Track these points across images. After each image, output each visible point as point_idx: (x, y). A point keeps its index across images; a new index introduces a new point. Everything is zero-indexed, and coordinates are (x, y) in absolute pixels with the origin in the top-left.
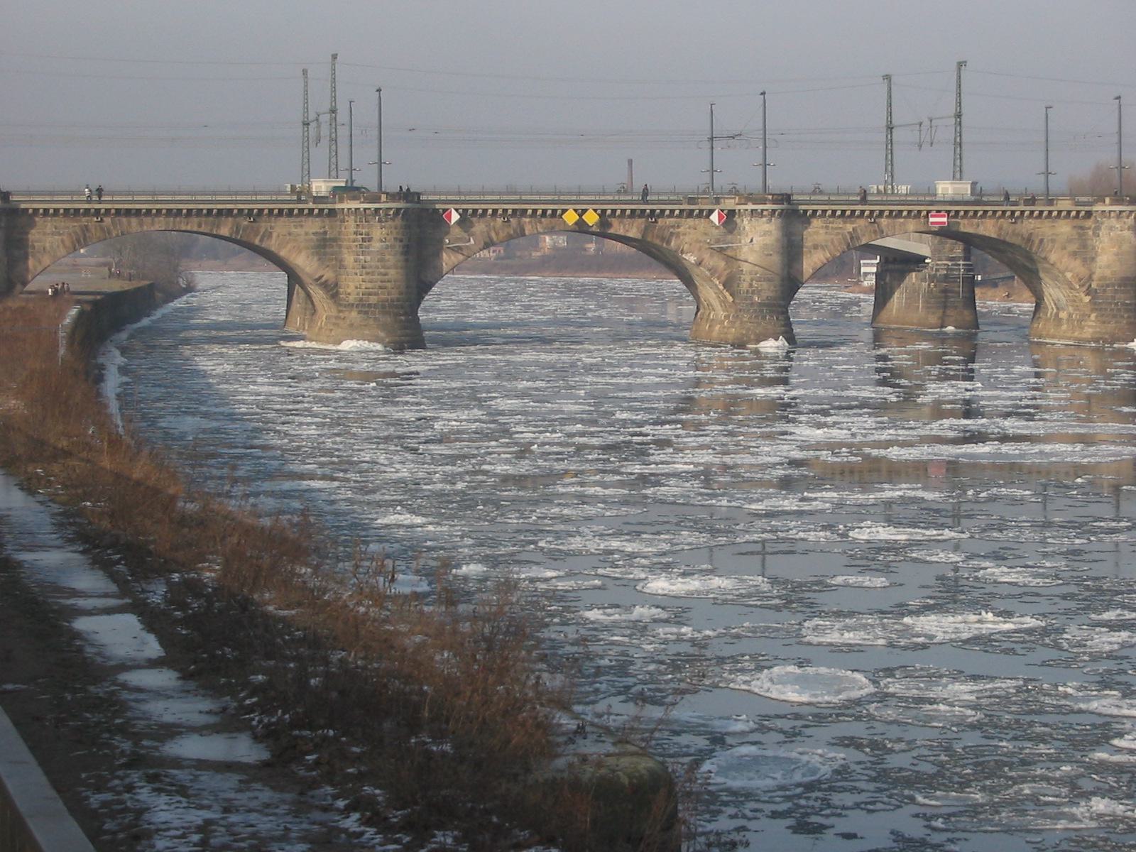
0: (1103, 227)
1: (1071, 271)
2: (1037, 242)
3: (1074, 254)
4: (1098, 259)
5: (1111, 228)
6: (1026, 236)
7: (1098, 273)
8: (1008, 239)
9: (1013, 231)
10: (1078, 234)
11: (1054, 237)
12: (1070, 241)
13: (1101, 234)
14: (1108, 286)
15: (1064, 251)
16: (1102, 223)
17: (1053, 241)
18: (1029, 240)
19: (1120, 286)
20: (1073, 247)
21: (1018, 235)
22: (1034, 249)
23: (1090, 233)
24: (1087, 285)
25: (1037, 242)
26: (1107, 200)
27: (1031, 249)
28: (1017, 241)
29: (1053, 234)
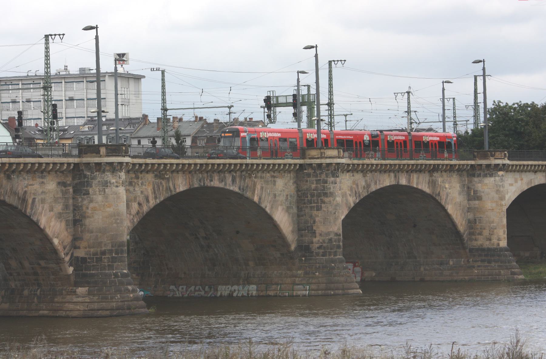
0: (95, 182)
1: (57, 237)
2: (30, 201)
3: (60, 216)
4: (87, 222)
5: (106, 184)
6: (21, 193)
7: (87, 236)
8: (7, 200)
9: (11, 189)
10: (62, 191)
11: (43, 196)
12: (56, 200)
13: (91, 191)
14: (104, 253)
15: (52, 213)
16: (92, 179)
17: (43, 201)
18: (24, 200)
19: (117, 253)
20: (59, 208)
21: (15, 194)
22: (28, 210)
23: (71, 190)
24: (70, 253)
25: (30, 201)
26: (103, 150)
27: (26, 211)
28: (12, 201)
29: (43, 192)
